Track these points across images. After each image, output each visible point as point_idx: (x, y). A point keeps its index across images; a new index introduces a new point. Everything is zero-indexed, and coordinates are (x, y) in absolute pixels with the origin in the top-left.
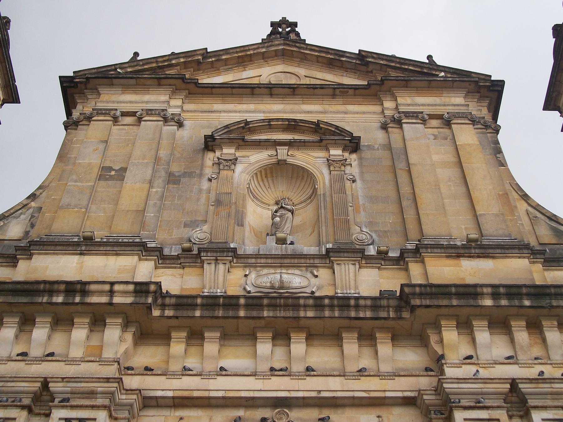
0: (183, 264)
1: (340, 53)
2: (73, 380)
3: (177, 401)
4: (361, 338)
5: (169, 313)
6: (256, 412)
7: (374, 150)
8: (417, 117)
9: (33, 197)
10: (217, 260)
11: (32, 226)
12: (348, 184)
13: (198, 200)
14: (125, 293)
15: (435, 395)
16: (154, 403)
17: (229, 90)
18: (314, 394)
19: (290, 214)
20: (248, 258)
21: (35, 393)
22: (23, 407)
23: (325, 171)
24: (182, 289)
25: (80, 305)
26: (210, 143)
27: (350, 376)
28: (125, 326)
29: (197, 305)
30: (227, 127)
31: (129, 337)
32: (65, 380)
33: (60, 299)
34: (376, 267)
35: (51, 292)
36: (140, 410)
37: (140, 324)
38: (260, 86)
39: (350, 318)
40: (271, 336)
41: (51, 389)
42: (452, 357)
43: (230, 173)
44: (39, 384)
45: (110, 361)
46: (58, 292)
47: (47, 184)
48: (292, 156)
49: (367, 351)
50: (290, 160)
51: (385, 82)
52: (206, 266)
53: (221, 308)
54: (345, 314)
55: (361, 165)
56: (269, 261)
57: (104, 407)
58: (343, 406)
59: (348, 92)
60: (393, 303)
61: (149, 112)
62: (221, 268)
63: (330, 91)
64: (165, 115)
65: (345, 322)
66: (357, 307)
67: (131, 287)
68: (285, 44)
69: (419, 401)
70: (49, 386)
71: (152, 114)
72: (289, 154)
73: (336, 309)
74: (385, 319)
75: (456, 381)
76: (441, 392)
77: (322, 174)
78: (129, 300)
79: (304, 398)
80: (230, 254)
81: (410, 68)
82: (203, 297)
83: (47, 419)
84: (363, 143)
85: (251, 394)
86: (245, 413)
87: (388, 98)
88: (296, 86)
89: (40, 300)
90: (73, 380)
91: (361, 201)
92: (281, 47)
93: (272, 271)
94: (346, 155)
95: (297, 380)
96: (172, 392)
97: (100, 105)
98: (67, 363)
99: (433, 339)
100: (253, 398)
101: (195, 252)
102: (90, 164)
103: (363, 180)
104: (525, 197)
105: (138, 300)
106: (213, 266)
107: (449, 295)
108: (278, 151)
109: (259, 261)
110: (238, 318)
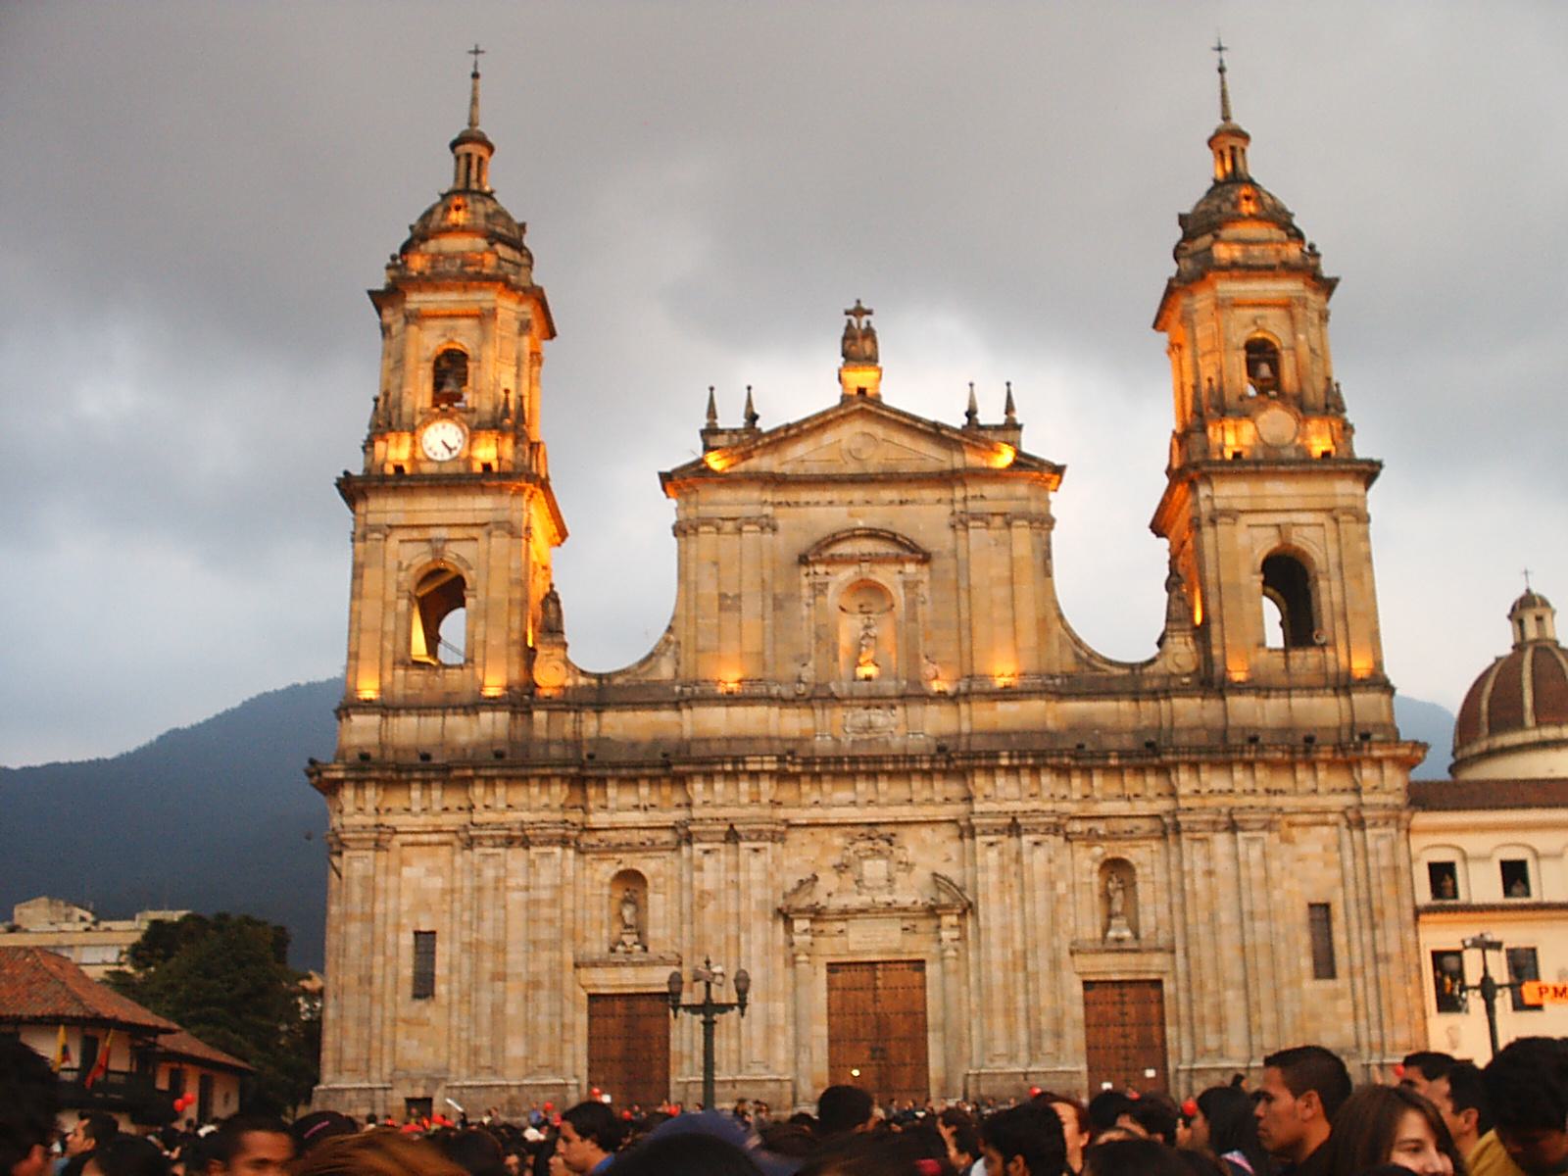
1: (918, 420)
5: (798, 769)
8: (981, 519)
9: (670, 629)
11: (678, 663)
12: (920, 608)
14: (772, 762)
23: (901, 592)
24: (802, 731)
28: (771, 778)
35: (723, 763)
42: (979, 797)
49: (927, 784)
50: (873, 577)
62: (827, 712)
66: (921, 761)
68: (863, 401)
78: (774, 767)
92: (859, 406)
99: (969, 781)
104: (1061, 617)
107: (980, 758)
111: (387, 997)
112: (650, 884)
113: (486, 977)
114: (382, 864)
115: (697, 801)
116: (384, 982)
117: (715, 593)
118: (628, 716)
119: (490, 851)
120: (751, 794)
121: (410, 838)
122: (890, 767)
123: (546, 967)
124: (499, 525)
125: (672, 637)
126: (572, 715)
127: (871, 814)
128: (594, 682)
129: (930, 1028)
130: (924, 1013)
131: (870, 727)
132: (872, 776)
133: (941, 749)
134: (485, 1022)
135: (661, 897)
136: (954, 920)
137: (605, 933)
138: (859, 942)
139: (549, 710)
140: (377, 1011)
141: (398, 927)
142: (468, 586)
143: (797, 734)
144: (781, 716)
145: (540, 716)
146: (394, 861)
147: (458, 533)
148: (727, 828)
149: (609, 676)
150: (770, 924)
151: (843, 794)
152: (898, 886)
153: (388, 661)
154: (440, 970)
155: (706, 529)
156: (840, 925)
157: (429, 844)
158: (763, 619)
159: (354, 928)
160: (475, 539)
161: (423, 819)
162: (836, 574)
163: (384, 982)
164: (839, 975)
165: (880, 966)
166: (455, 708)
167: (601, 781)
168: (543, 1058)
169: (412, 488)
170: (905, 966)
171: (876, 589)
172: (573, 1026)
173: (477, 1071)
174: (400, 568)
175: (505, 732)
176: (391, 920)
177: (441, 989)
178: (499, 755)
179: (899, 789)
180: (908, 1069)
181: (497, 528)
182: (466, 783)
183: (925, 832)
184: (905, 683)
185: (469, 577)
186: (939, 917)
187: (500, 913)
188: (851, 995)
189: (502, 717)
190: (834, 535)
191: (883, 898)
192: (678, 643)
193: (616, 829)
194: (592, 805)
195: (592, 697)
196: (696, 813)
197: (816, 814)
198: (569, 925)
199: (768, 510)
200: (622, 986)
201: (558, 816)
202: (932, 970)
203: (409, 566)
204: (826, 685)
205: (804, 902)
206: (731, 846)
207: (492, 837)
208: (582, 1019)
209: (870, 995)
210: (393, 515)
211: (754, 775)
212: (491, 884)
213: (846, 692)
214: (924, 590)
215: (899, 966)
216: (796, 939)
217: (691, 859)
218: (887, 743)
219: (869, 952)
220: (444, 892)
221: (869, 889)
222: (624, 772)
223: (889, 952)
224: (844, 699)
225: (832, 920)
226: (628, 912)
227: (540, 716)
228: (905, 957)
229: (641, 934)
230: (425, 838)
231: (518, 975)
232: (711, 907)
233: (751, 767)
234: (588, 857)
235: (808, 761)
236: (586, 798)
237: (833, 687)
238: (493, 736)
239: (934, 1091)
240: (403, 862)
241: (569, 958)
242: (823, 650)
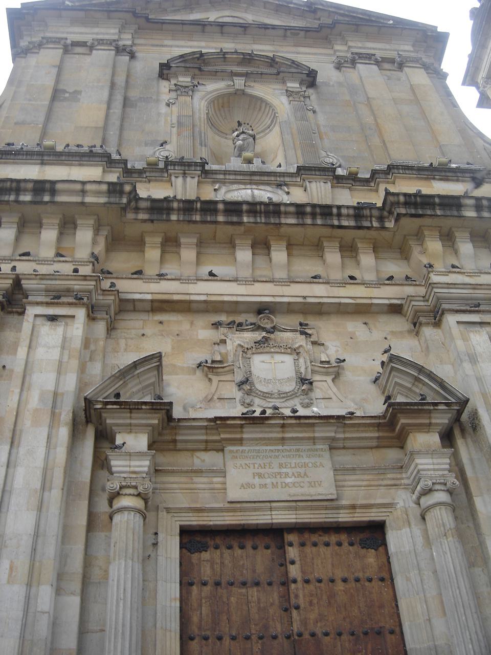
0: (149, 178)
2: (48, 277)
3: (156, 304)
4: (342, 248)
5: (142, 216)
6: (239, 318)
7: (330, 86)
8: (370, 59)
10: (185, 174)
14: (98, 193)
15: (424, 301)
16: (131, 307)
17: (179, 27)
19: (251, 139)
20: (216, 174)
21: (7, 291)
25: (49, 204)
26: (165, 72)
27: (334, 283)
29: (173, 209)
30: (181, 56)
31: (102, 241)
32: (38, 277)
33: (27, 198)
34: (347, 188)
36: (116, 314)
37: (112, 228)
38: (211, 24)
39: (333, 226)
40: (251, 243)
41: (23, 285)
43: (189, 99)
44: (11, 281)
45: (84, 262)
46: (26, 190)
48: (250, 86)
51: (337, 25)
52: (173, 178)
53: (198, 213)
54: (329, 222)
56: (239, 177)
58: (328, 313)
59: (298, 34)
60: (375, 213)
61: (101, 42)
63: (281, 32)
64: (117, 45)
65: (326, 231)
67: (104, 187)
69: (405, 308)
70: (22, 283)
71: (103, 44)
72: (246, 85)
73: (318, 217)
74: (368, 228)
75: (446, 286)
76: (429, 298)
78: (103, 200)
79: (289, 303)
80: (198, 168)
81: (358, 16)
82: (179, 201)
83: (21, 317)
84: (319, 79)
85: (234, 299)
86: (227, 318)
87: (338, 42)
88: (247, 25)
89: (6, 198)
90: (48, 277)
93: (243, 187)
95: (280, 287)
96: (150, 295)
97: (49, 35)
98: (37, 262)
100: (237, 303)
101: (161, 165)
105: (112, 200)
106: (180, 180)
108: (235, 81)
109: (227, 177)
110: (216, 222)
136: (434, 439)
138: (249, 486)
156: (208, 459)
164: (205, 555)
170: (343, 537)
183: (354, 326)
188: (235, 597)
209: (274, 595)
215: (333, 538)
216: (117, 464)
228: (344, 517)
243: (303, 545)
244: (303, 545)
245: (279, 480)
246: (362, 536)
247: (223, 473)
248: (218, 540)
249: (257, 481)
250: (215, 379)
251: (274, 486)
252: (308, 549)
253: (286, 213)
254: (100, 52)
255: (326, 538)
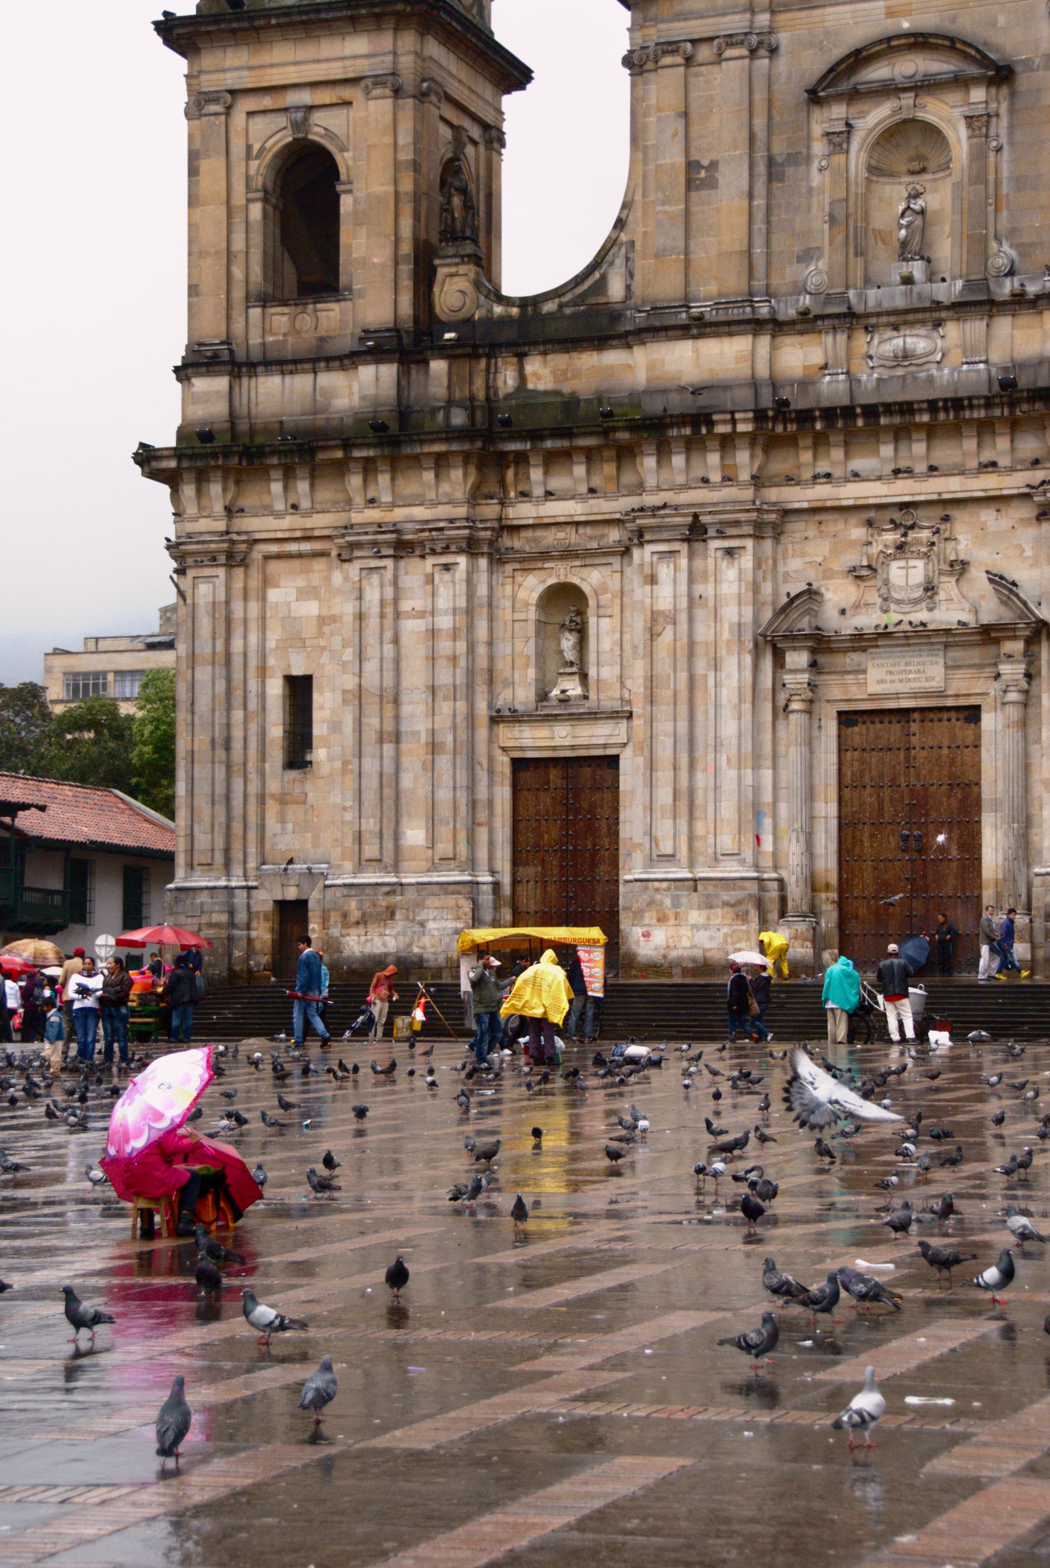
7: (1033, 70)
9: (620, 224)
11: (631, 275)
13: (809, 208)
14: (745, 420)
18: (935, 497)
22: (683, 540)
23: (963, 132)
24: (805, 368)
28: (753, 445)
31: (759, 453)
47: (629, 198)
50: (921, 115)
55: (1012, 111)
57: (750, 536)
66: (971, 407)
67: (750, 415)
77: (959, 140)
82: (821, 410)
91: (1005, 189)
94: (993, 91)
102: (673, 165)
103: (1011, 144)
111: (252, 765)
112: (592, 603)
113: (370, 736)
114: (238, 585)
115: (651, 481)
116: (245, 748)
117: (680, 160)
118: (559, 360)
119: (374, 563)
120: (723, 467)
121: (274, 548)
122: (925, 418)
123: (448, 723)
124: (378, 80)
125: (624, 237)
126: (483, 363)
127: (903, 490)
128: (515, 311)
129: (984, 804)
130: (978, 784)
131: (906, 355)
132: (901, 434)
133: (1008, 385)
134: (370, 797)
135: (607, 620)
137: (531, 673)
138: (883, 681)
139: (451, 358)
140: (238, 784)
141: (263, 671)
142: (343, 177)
143: (798, 373)
144: (773, 348)
145: (438, 366)
146: (254, 582)
147: (325, 96)
148: (690, 519)
149: (537, 300)
150: (748, 659)
151: (861, 463)
152: (942, 595)
153: (238, 294)
154: (318, 730)
155: (668, 60)
156: (853, 659)
157: (300, 556)
158: (751, 197)
159: (203, 674)
160: (348, 103)
161: (288, 522)
162: (862, 115)
163: (245, 748)
164: (856, 729)
165: (916, 716)
166: (328, 359)
167: (521, 460)
168: (444, 848)
169: (257, 29)
170: (953, 715)
171: (932, 133)
172: (491, 803)
173: (360, 865)
174: (248, 156)
175: (393, 393)
176: (253, 662)
177: (319, 754)
178: (379, 428)
179: (946, 453)
180: (954, 864)
181: (376, 84)
182: (340, 468)
183: (987, 515)
184: (959, 284)
185: (344, 160)
186: (997, 642)
187: (389, 649)
188: (874, 758)
189: (388, 372)
190: (857, 52)
191: (921, 615)
192: (632, 243)
193: (548, 525)
194: (512, 494)
195: (509, 334)
196: (650, 500)
197: (822, 493)
198: (482, 663)
199: (763, 19)
200: (554, 748)
201: (462, 511)
202: (988, 720)
203: (262, 149)
204: (843, 297)
205: (805, 625)
206: (698, 546)
207: (375, 543)
208: (503, 794)
210: (235, 74)
211: (727, 443)
212: (375, 610)
213: (871, 304)
214: (1001, 126)
216: (788, 678)
217: (642, 565)
218: (931, 379)
219: (897, 696)
220: (322, 621)
221: (899, 602)
222: (549, 444)
223: (927, 695)
224: (868, 315)
225: (845, 651)
226: (568, 642)
227: (438, 366)
228: (950, 702)
229: (584, 677)
230: (293, 547)
231: (416, 734)
232: (667, 636)
233: (722, 429)
234: (509, 568)
235: (805, 417)
236: (502, 483)
237: (852, 294)
238: (376, 397)
239: (988, 896)
240: (266, 582)
241: (482, 708)
242: (840, 239)
243: (922, 721)
244: (922, 721)
245: (904, 676)
246: (966, 713)
247: (864, 672)
248: (865, 718)
249: (889, 677)
250: (862, 584)
251: (901, 681)
252: (928, 724)
253: (921, 411)
254: (732, 63)
255: (939, 715)
